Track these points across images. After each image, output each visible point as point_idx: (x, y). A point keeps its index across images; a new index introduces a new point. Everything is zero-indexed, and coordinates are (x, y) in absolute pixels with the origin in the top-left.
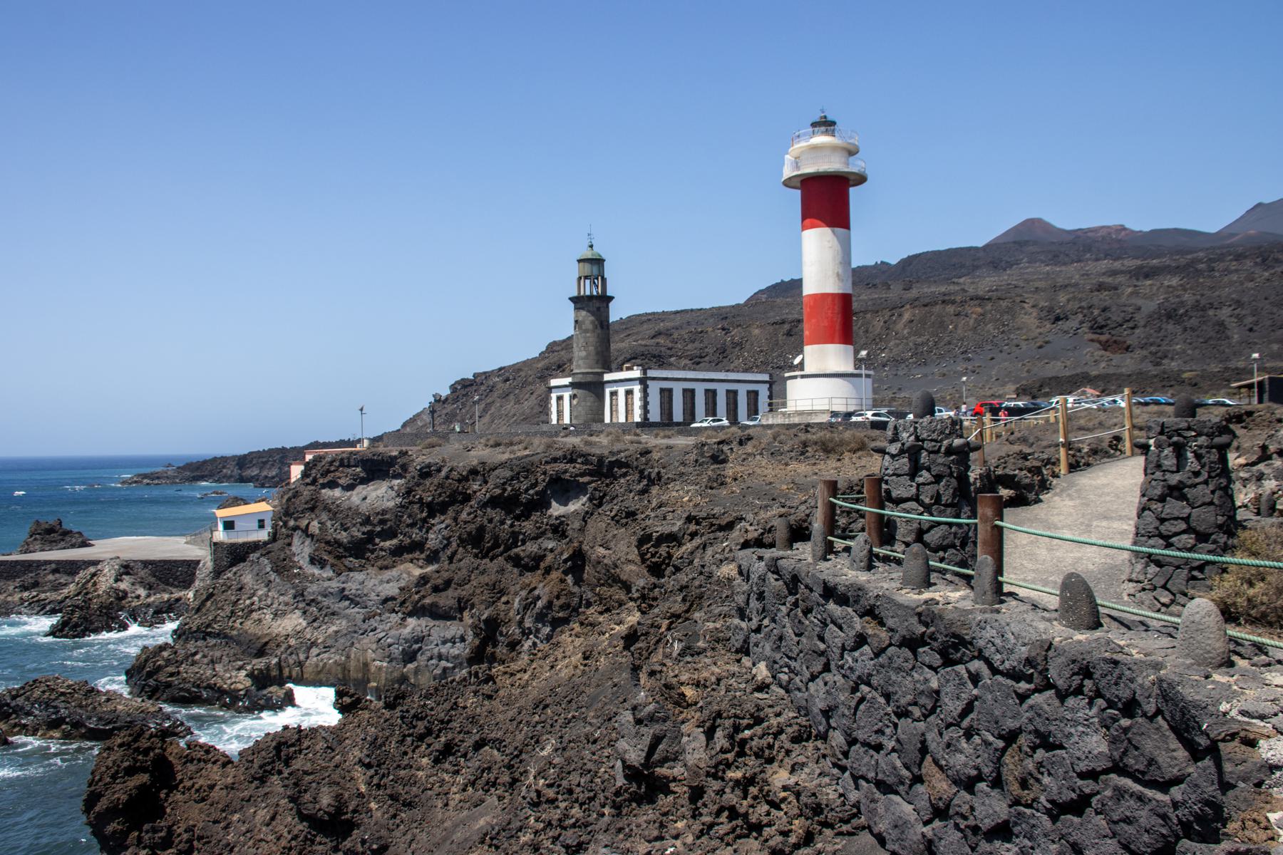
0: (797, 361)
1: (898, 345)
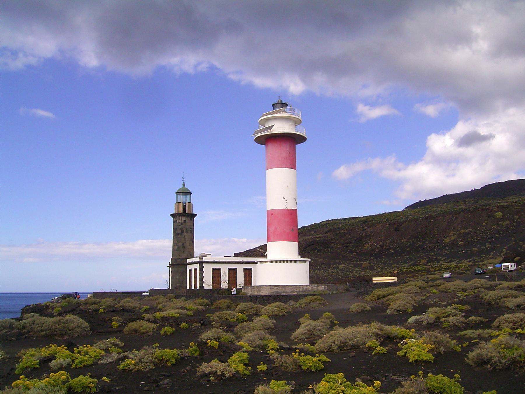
1: (454, 235)
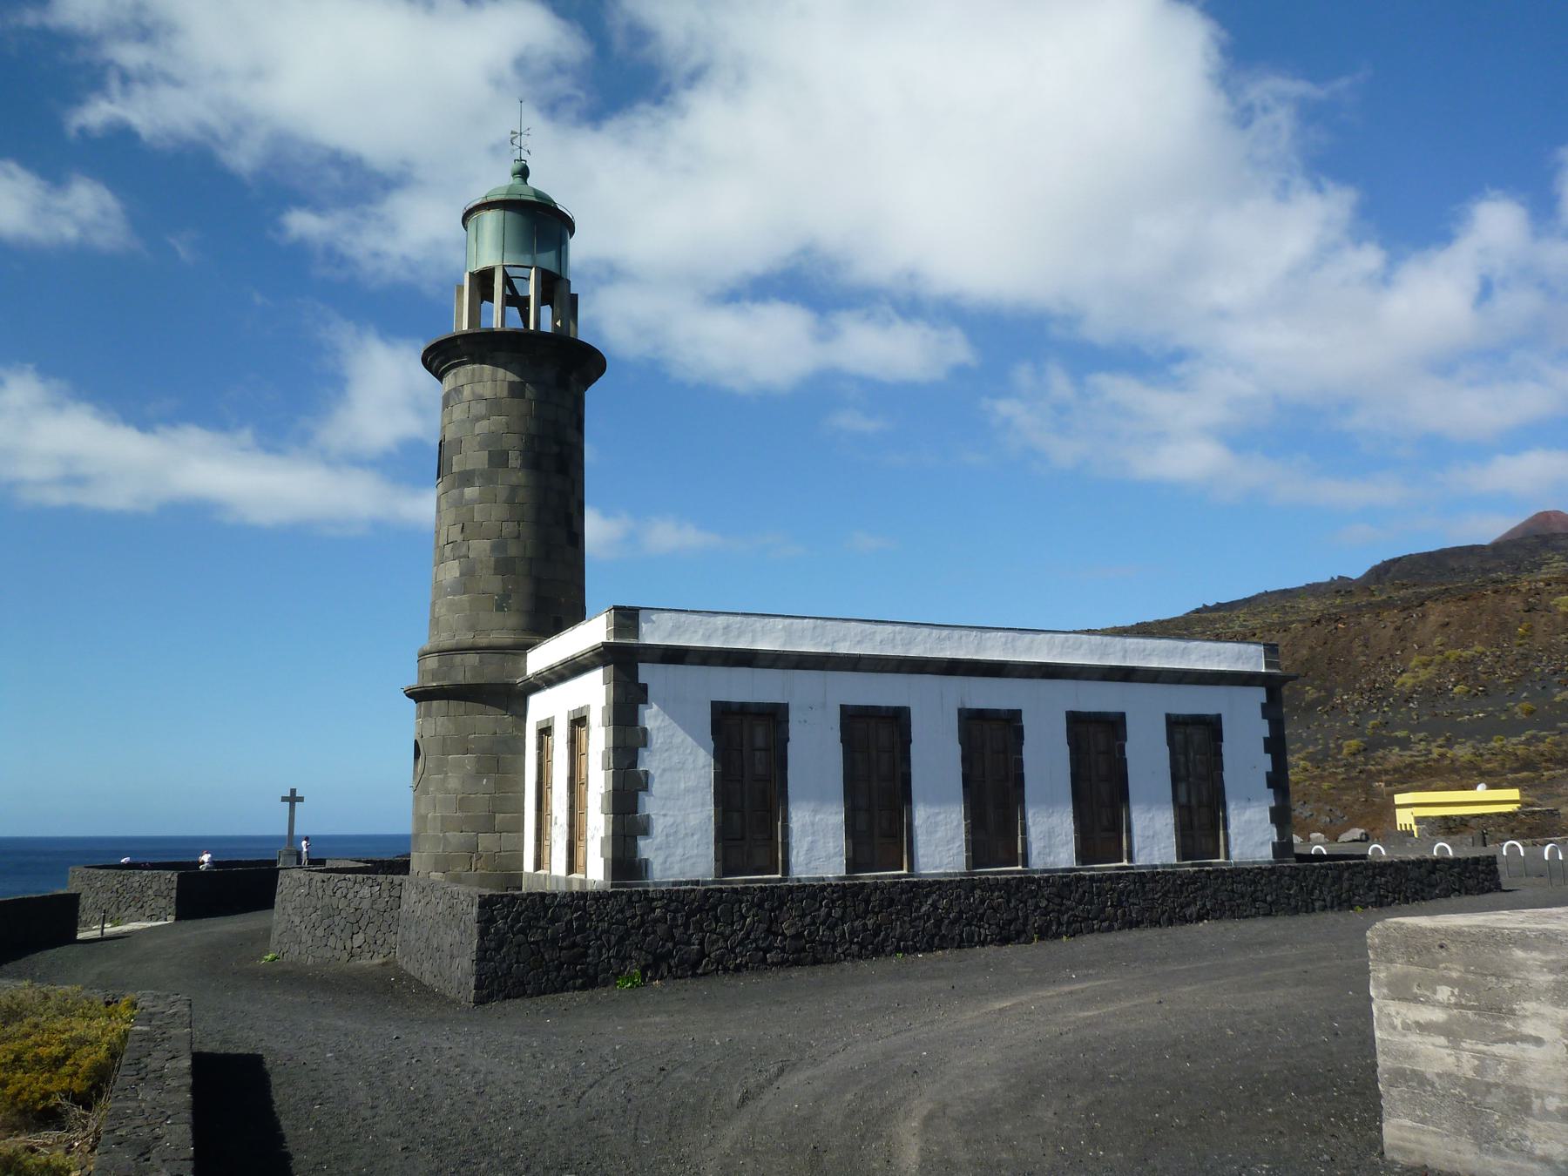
1: (1425, 665)
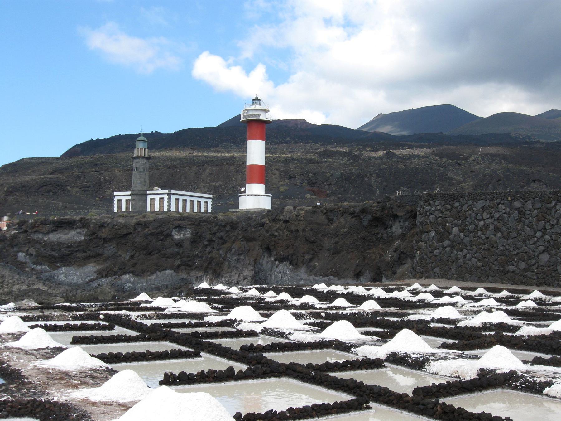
0: (243, 190)
